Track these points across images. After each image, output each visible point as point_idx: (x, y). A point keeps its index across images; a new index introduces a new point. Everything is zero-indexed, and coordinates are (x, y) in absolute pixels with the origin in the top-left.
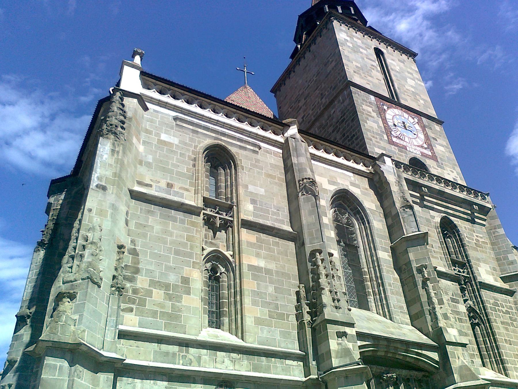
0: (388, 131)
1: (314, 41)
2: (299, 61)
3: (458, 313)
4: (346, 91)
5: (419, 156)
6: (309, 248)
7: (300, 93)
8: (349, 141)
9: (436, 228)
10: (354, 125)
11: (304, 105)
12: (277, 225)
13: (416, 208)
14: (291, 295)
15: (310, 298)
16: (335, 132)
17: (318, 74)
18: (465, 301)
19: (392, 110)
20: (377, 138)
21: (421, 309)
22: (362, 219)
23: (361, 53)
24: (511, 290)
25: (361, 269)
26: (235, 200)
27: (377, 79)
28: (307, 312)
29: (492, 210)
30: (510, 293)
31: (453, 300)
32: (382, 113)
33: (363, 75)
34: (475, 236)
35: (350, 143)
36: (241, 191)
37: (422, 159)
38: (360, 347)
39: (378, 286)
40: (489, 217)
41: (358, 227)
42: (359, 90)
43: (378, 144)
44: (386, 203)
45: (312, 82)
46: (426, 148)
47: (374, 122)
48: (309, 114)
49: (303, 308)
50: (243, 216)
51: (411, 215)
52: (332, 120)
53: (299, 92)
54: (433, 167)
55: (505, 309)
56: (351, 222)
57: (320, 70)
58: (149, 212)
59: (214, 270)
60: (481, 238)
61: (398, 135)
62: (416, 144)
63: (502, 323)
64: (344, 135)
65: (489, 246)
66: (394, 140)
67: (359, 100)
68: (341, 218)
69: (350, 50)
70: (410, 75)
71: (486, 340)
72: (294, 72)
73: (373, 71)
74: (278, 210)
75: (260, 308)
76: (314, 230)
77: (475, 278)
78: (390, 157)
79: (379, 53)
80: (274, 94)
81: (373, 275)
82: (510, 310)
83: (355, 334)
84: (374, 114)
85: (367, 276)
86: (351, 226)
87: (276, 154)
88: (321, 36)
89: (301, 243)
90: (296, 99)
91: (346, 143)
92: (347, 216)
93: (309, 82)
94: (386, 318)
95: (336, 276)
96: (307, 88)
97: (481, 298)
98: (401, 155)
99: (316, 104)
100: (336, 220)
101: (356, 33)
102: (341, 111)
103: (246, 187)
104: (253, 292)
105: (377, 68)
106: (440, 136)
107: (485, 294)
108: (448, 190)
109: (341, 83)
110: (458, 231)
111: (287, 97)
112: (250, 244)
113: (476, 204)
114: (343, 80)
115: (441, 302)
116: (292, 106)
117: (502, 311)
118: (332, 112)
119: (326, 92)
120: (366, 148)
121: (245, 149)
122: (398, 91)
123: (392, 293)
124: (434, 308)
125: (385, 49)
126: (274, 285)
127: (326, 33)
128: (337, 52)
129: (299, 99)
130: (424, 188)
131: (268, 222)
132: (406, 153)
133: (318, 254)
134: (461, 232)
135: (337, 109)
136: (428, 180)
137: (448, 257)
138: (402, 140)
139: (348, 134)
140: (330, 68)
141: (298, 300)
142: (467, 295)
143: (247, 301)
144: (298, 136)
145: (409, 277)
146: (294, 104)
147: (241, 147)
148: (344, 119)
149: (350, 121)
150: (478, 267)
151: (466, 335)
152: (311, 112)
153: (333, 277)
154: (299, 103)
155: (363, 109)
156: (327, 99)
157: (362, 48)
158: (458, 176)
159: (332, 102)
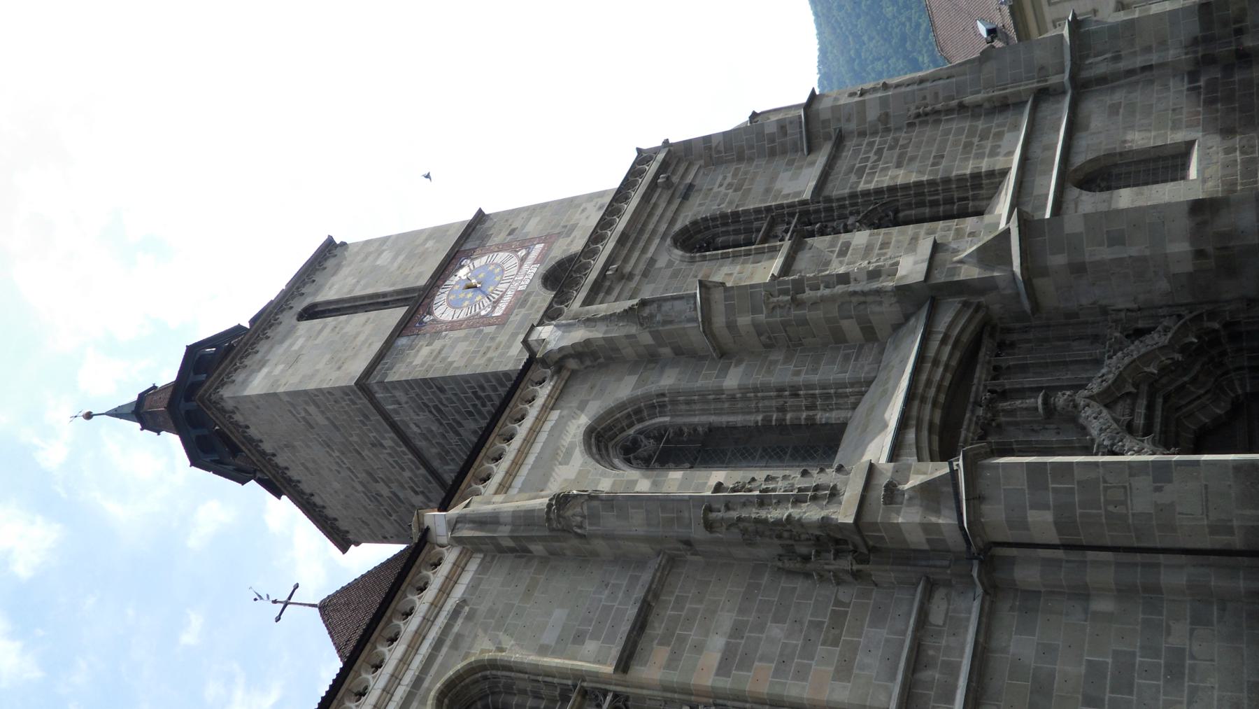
0: (476, 323)
1: (254, 443)
2: (290, 480)
3: (868, 249)
4: (376, 392)
5: (543, 269)
6: (698, 533)
7: (360, 488)
8: (484, 405)
9: (692, 261)
10: (453, 389)
11: (390, 487)
12: (639, 593)
13: (646, 294)
14: (796, 588)
15: (803, 550)
16: (461, 430)
17: (329, 446)
18: (847, 231)
20: (489, 348)
21: (854, 321)
22: (653, 406)
23: (302, 348)
24: (837, 138)
25: (757, 426)
26: (570, 682)
27: (364, 324)
28: (835, 559)
29: (672, 148)
30: (840, 140)
31: (843, 253)
34: (719, 189)
35: (489, 403)
37: (551, 262)
38: (920, 459)
39: (797, 395)
40: (685, 156)
41: (667, 419)
42: (379, 367)
43: (502, 346)
44: (628, 351)
45: (342, 461)
46: (528, 254)
47: (453, 347)
48: (411, 478)
49: (827, 567)
50: (608, 669)
51: (660, 307)
52: (432, 431)
53: (356, 491)
54: (569, 245)
55: (872, 155)
56: (656, 432)
57: (320, 440)
60: (725, 178)
61: (489, 303)
62: (514, 271)
64: (470, 413)
65: (743, 166)
66: (498, 312)
67: (402, 370)
68: (645, 451)
69: (290, 371)
70: (371, 258)
71: (930, 201)
72: (312, 495)
73: (345, 331)
74: (607, 585)
75: (814, 663)
76: (661, 515)
77: (804, 203)
78: (533, 327)
79: (311, 313)
80: (353, 546)
81: (774, 403)
82: (876, 147)
83: (892, 464)
84: (437, 344)
85: (774, 418)
86: (663, 432)
87: (483, 569)
88: (247, 427)
89: (685, 547)
90: (371, 501)
91: (489, 412)
92: (642, 437)
93: (340, 466)
94: (866, 392)
95: (765, 485)
96: (352, 472)
97: (844, 199)
98: (532, 305)
99: (391, 460)
101: (257, 352)
102: (417, 410)
104: (777, 673)
105: (340, 322)
106: (507, 221)
107: (838, 189)
108: (621, 224)
109: (358, 401)
110: (705, 220)
111: (363, 519)
112: (671, 664)
113: (656, 176)
114: (352, 397)
116: (388, 512)
117: (875, 161)
118: (416, 429)
119: (371, 435)
120: (506, 374)
121: (459, 636)
122: (399, 287)
123: (815, 371)
124: (855, 293)
125: (305, 298)
126: (769, 624)
127: (242, 414)
128: (289, 400)
129: (374, 494)
130: (608, 270)
131: (629, 612)
132: (529, 294)
133: (713, 515)
134: (708, 215)
135: (411, 419)
136: (594, 260)
137: (755, 249)
138: (502, 297)
139: (468, 404)
140: (321, 420)
141: (808, 575)
142: (835, 224)
143: (794, 690)
144: (455, 512)
145: (786, 331)
146: (382, 508)
147: (455, 646)
148: (436, 407)
149: (442, 396)
150: (782, 194)
151: (915, 239)
152: (407, 474)
153: (766, 490)
154: (382, 496)
155: (422, 365)
156: (386, 435)
158: (595, 200)
159: (394, 426)
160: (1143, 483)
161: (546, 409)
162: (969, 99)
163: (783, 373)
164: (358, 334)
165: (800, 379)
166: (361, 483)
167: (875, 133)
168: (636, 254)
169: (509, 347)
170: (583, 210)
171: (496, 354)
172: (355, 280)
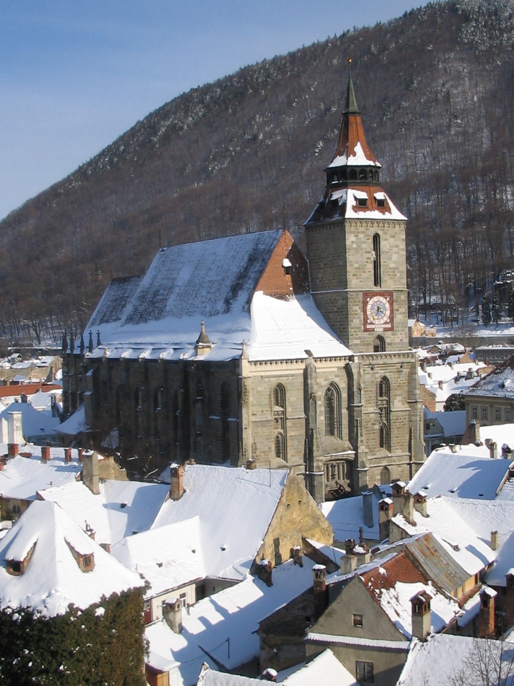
5: (381, 334)
19: (372, 299)
23: (362, 249)
32: (365, 304)
33: (358, 274)
36: (287, 404)
58: (257, 427)
59: (277, 437)
62: (382, 322)
63: (397, 428)
66: (368, 327)
77: (390, 408)
84: (359, 311)
100: (326, 395)
103: (289, 399)
106: (403, 304)
112: (291, 427)
115: (361, 436)
143: (288, 449)
155: (353, 311)
157: (363, 243)
160: (320, 496)
161: (337, 367)
162: (413, 441)
163: (345, 421)
164: (364, 272)
165: (343, 426)
166: (323, 258)
167: (409, 418)
168: (379, 368)
169: (357, 339)
170: (401, 334)
171: (355, 336)
172: (387, 250)
